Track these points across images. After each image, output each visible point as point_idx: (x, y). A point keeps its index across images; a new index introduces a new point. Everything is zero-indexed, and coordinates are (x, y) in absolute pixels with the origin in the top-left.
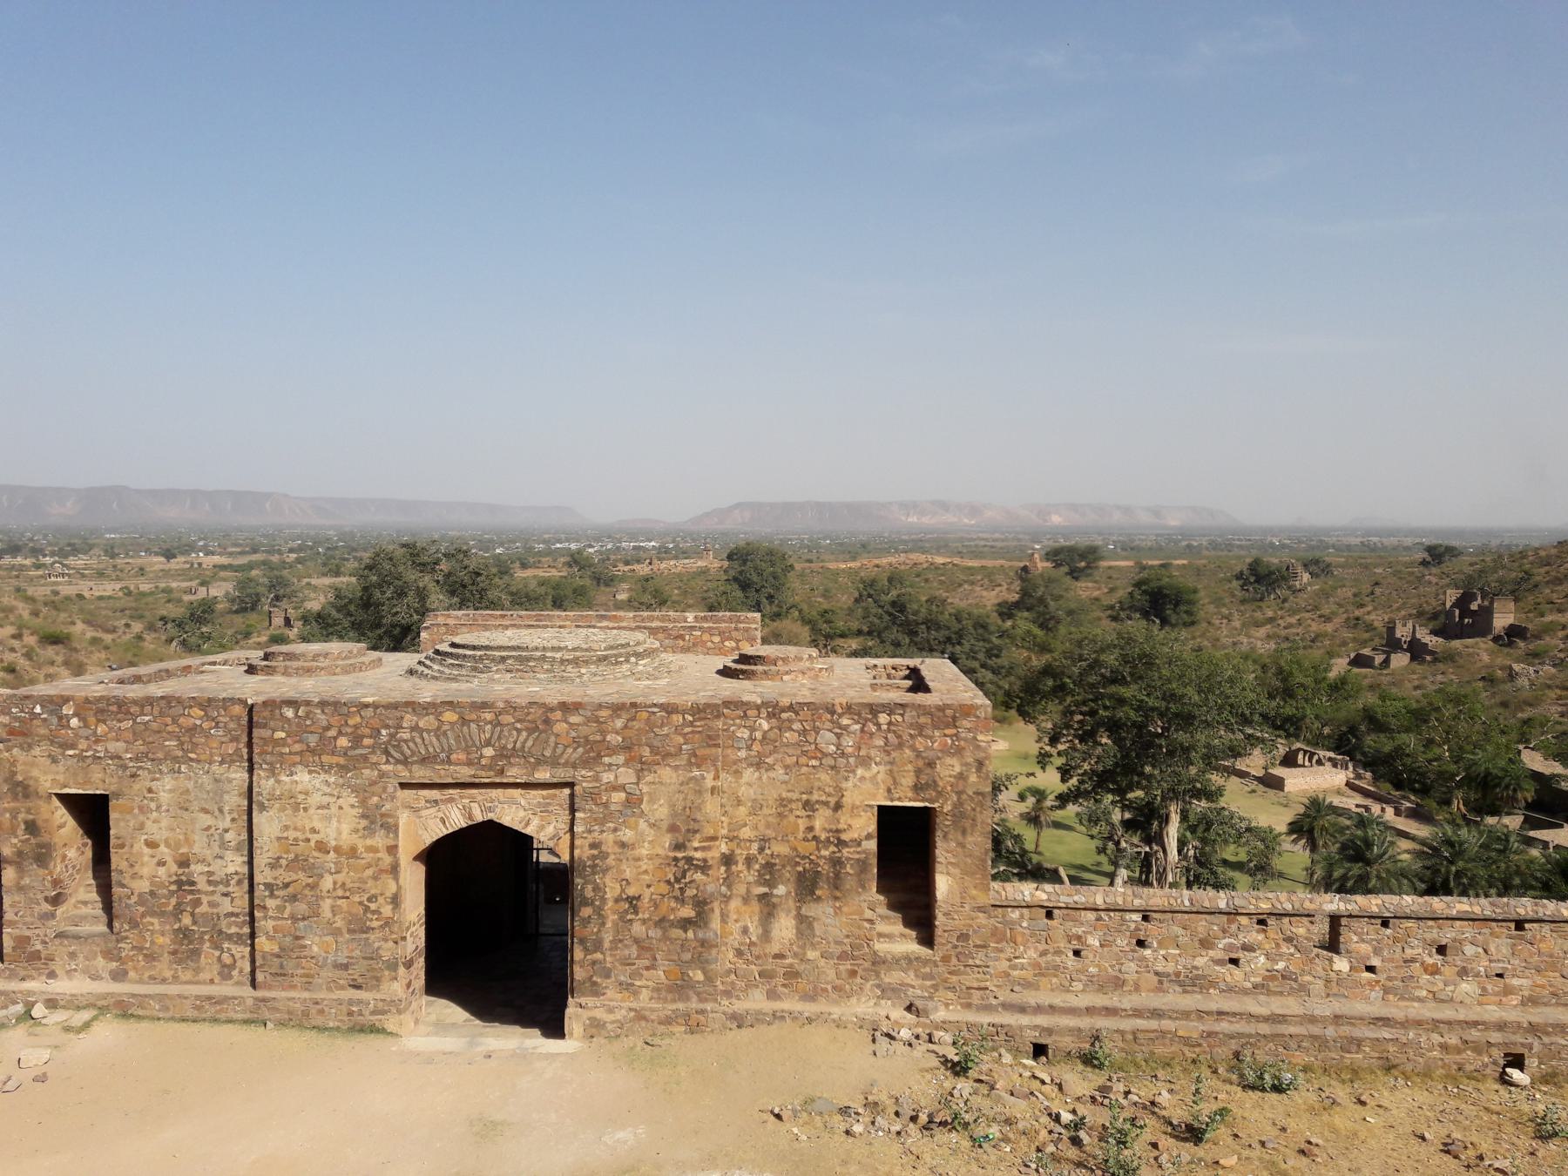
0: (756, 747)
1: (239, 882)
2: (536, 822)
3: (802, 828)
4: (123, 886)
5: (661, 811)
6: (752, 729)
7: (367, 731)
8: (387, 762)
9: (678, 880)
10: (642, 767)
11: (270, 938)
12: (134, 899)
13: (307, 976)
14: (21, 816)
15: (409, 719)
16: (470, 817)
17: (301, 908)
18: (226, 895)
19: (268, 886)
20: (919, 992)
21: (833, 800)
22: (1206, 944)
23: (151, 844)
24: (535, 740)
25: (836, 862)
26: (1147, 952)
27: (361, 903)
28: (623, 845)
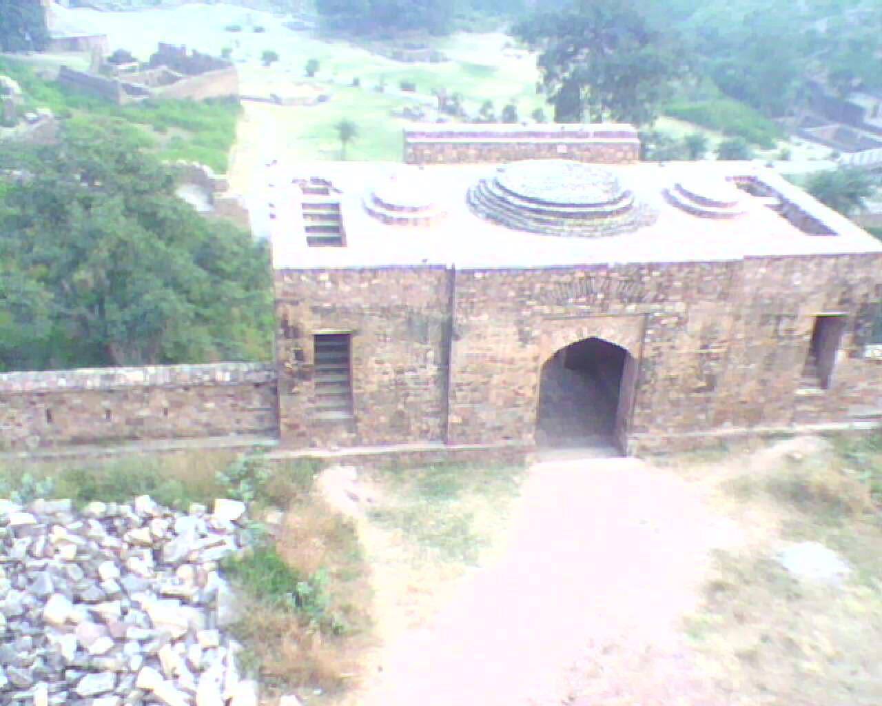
2: (619, 337)
5: (696, 326)
8: (538, 305)
11: (456, 414)
14: (292, 349)
15: (554, 277)
16: (581, 335)
17: (477, 395)
18: (426, 389)
19: (458, 385)
24: (629, 288)
27: (514, 391)
28: (673, 347)
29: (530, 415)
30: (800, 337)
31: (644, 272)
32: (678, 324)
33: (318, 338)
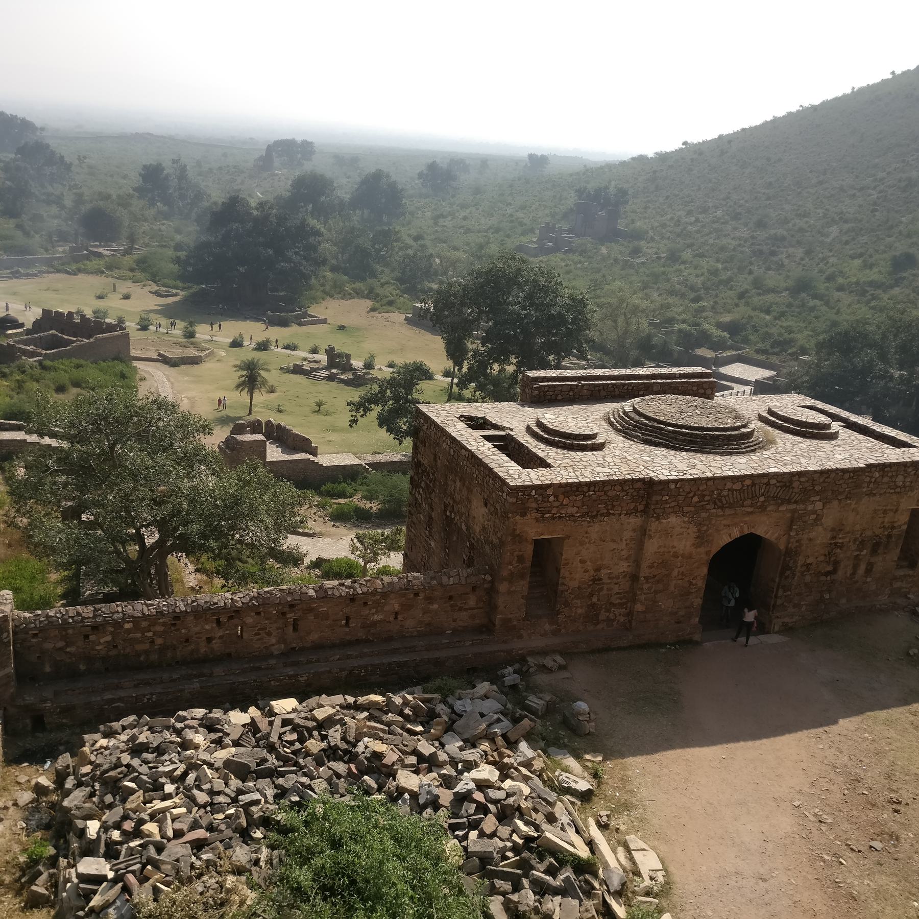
0: (871, 485)
1: (625, 576)
4: (563, 584)
6: (872, 477)
7: (707, 493)
9: (829, 554)
10: (826, 502)
12: (569, 591)
14: (516, 553)
17: (660, 586)
23: (582, 562)
25: (889, 536)
28: (810, 540)
29: (698, 601)
30: (900, 526)
31: (795, 479)
32: (815, 520)
33: (537, 542)
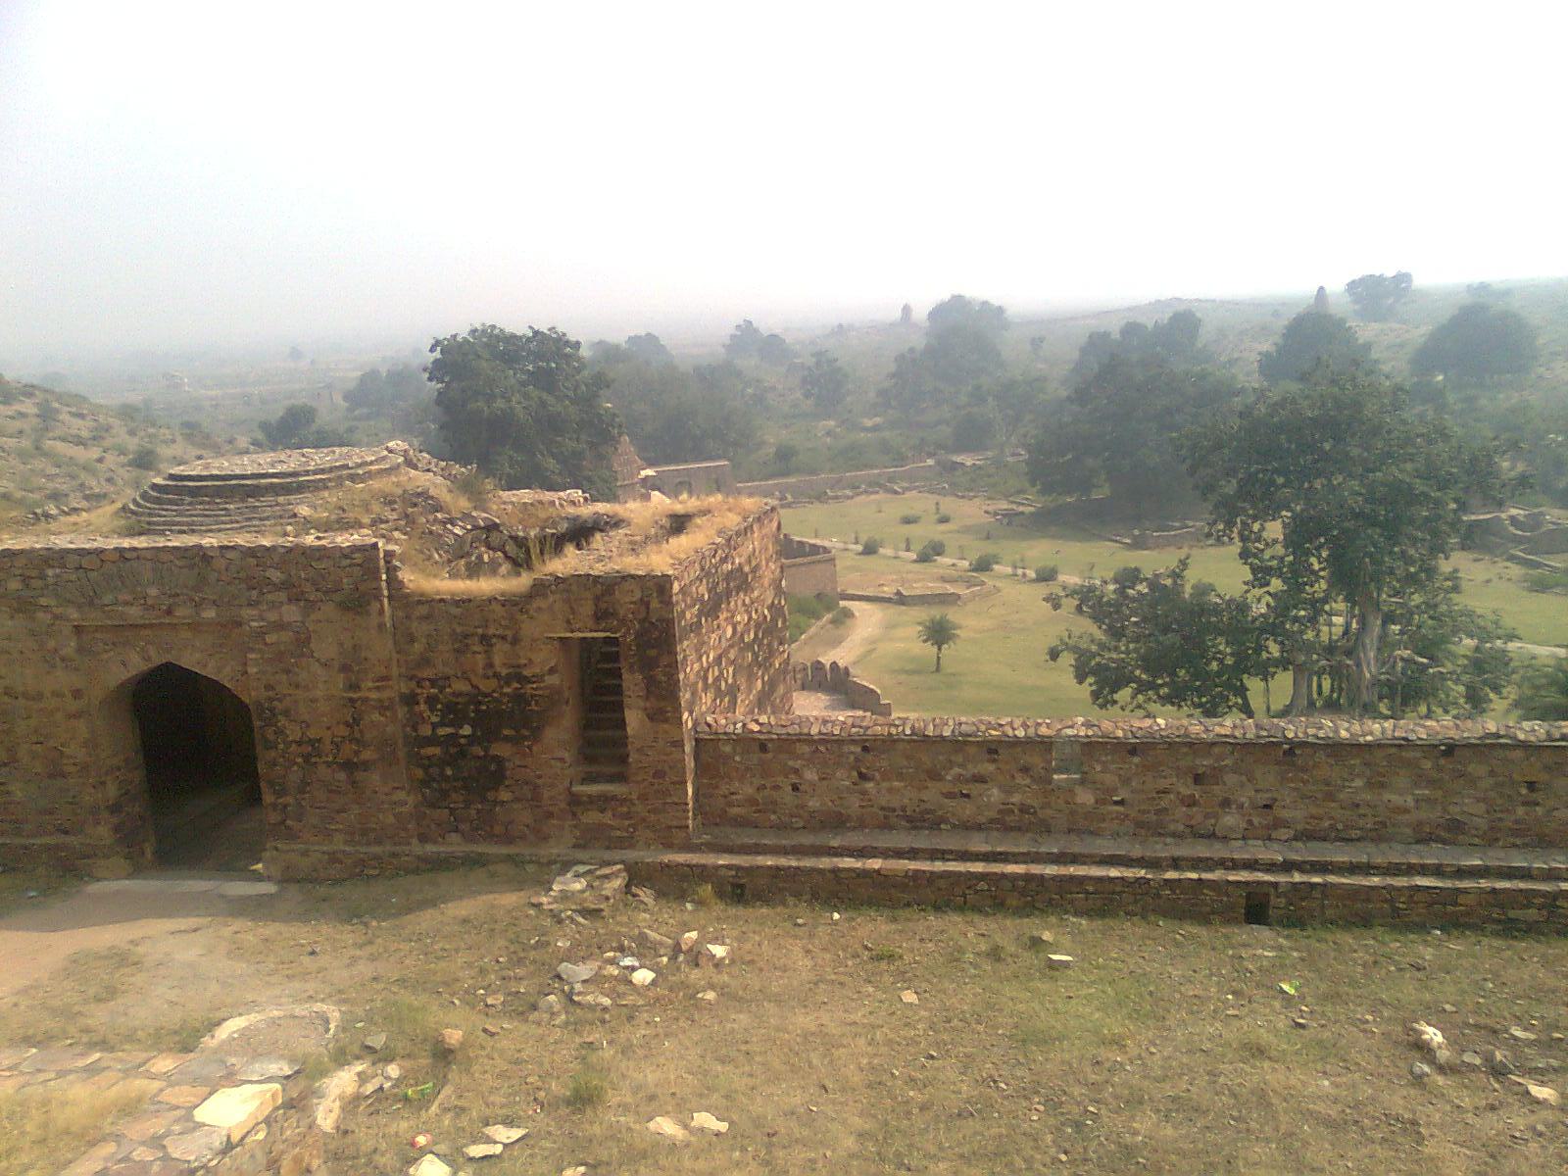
2: (212, 664)
3: (481, 665)
13: (16, 821)
16: (148, 659)
20: (618, 833)
21: (509, 633)
22: (934, 775)
26: (870, 785)
30: (539, 678)
